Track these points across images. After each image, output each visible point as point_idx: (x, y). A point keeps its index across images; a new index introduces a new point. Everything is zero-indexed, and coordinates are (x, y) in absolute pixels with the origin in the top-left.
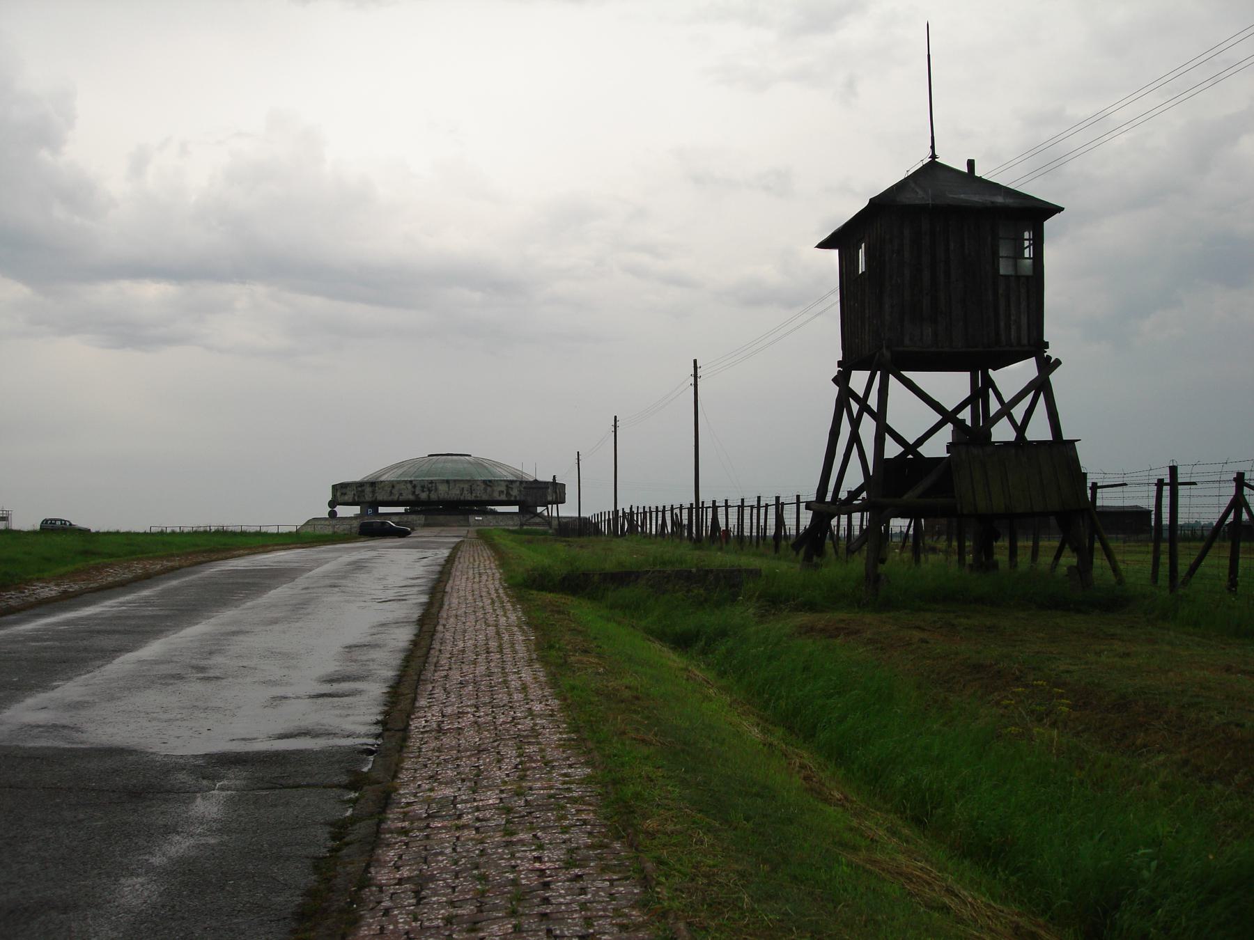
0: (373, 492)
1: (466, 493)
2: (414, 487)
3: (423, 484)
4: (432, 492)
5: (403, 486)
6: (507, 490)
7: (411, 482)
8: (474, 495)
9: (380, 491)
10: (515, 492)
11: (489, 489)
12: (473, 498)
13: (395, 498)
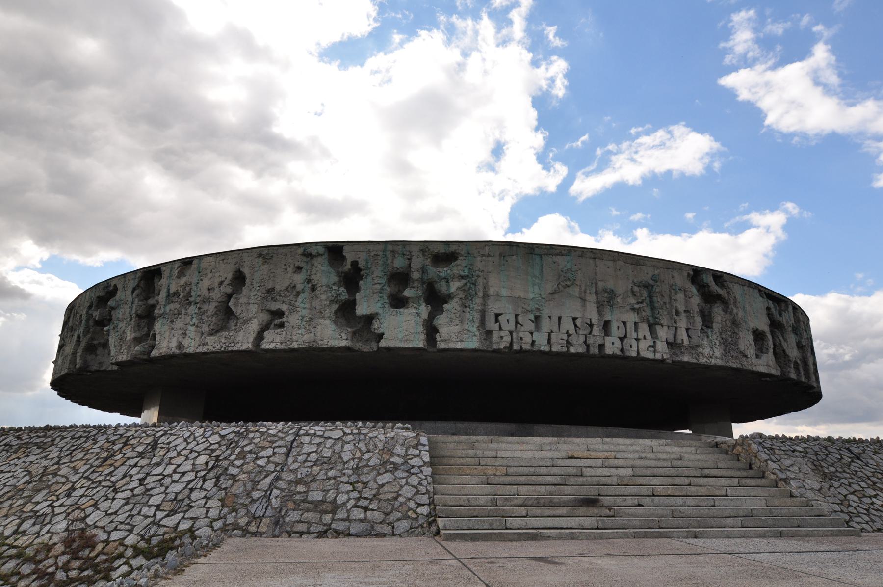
0: (147, 317)
1: (632, 318)
3: (399, 263)
8: (663, 333)
12: (662, 351)
13: (243, 341)
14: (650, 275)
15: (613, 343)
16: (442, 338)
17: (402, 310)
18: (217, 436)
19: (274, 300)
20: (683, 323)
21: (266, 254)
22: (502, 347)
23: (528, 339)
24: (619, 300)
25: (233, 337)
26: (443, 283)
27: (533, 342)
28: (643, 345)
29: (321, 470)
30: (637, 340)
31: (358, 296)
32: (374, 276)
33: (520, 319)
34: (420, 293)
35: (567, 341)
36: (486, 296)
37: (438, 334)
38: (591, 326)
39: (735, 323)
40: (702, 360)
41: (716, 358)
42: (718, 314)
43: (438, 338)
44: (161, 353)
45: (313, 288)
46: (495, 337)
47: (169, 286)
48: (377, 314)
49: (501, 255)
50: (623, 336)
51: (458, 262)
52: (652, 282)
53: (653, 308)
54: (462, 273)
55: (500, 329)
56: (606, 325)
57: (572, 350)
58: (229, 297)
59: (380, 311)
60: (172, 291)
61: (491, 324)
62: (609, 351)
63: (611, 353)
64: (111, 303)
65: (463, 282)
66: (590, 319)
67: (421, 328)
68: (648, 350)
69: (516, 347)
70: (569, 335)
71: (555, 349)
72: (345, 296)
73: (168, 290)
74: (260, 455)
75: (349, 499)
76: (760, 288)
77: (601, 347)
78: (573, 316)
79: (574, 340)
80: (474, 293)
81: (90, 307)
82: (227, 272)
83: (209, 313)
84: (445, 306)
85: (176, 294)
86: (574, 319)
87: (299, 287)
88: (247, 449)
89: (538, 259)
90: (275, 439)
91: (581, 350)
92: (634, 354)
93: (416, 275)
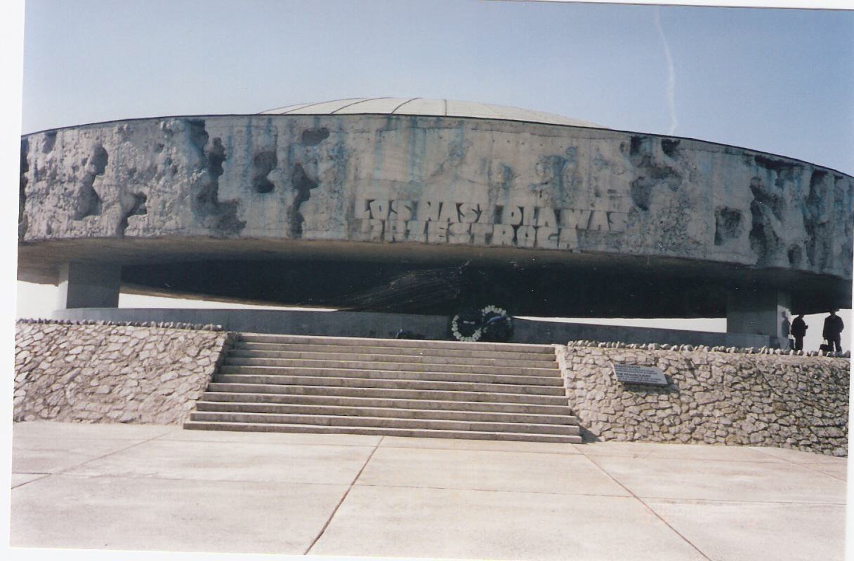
1: (529, 201)
6: (755, 210)
7: (196, 125)
8: (571, 219)
9: (42, 184)
10: (789, 229)
12: (570, 238)
14: (565, 147)
15: (504, 233)
16: (307, 228)
17: (268, 195)
18: (41, 333)
19: (136, 182)
22: (372, 238)
23: (401, 227)
24: (517, 181)
25: (97, 223)
26: (311, 165)
27: (407, 233)
28: (544, 233)
29: (117, 367)
30: (536, 228)
31: (221, 179)
32: (237, 156)
33: (394, 206)
34: (285, 177)
35: (448, 229)
36: (356, 178)
37: (303, 223)
38: (479, 212)
39: (686, 203)
40: (625, 249)
41: (647, 246)
42: (661, 195)
43: (303, 228)
44: (33, 237)
45: (175, 171)
46: (364, 227)
47: (36, 161)
48: (239, 199)
49: (377, 131)
50: (517, 222)
51: (329, 139)
52: (566, 157)
53: (562, 189)
54: (331, 154)
55: (371, 217)
56: (499, 211)
57: (453, 240)
58: (93, 176)
59: (243, 197)
60: (39, 168)
61: (361, 212)
62: (497, 241)
63: (500, 243)
65: (332, 163)
66: (478, 206)
67: (284, 216)
68: (549, 238)
69: (388, 237)
70: (450, 225)
71: (432, 239)
73: (36, 168)
74: (71, 352)
75: (131, 392)
76: (746, 152)
77: (489, 237)
78: (459, 201)
79: (456, 228)
80: (343, 176)
82: (86, 148)
83: (75, 194)
84: (312, 191)
85: (44, 171)
86: (458, 206)
87: (160, 168)
88: (62, 346)
89: (419, 133)
90: (88, 337)
91: (463, 240)
92: (530, 244)
93: (281, 156)
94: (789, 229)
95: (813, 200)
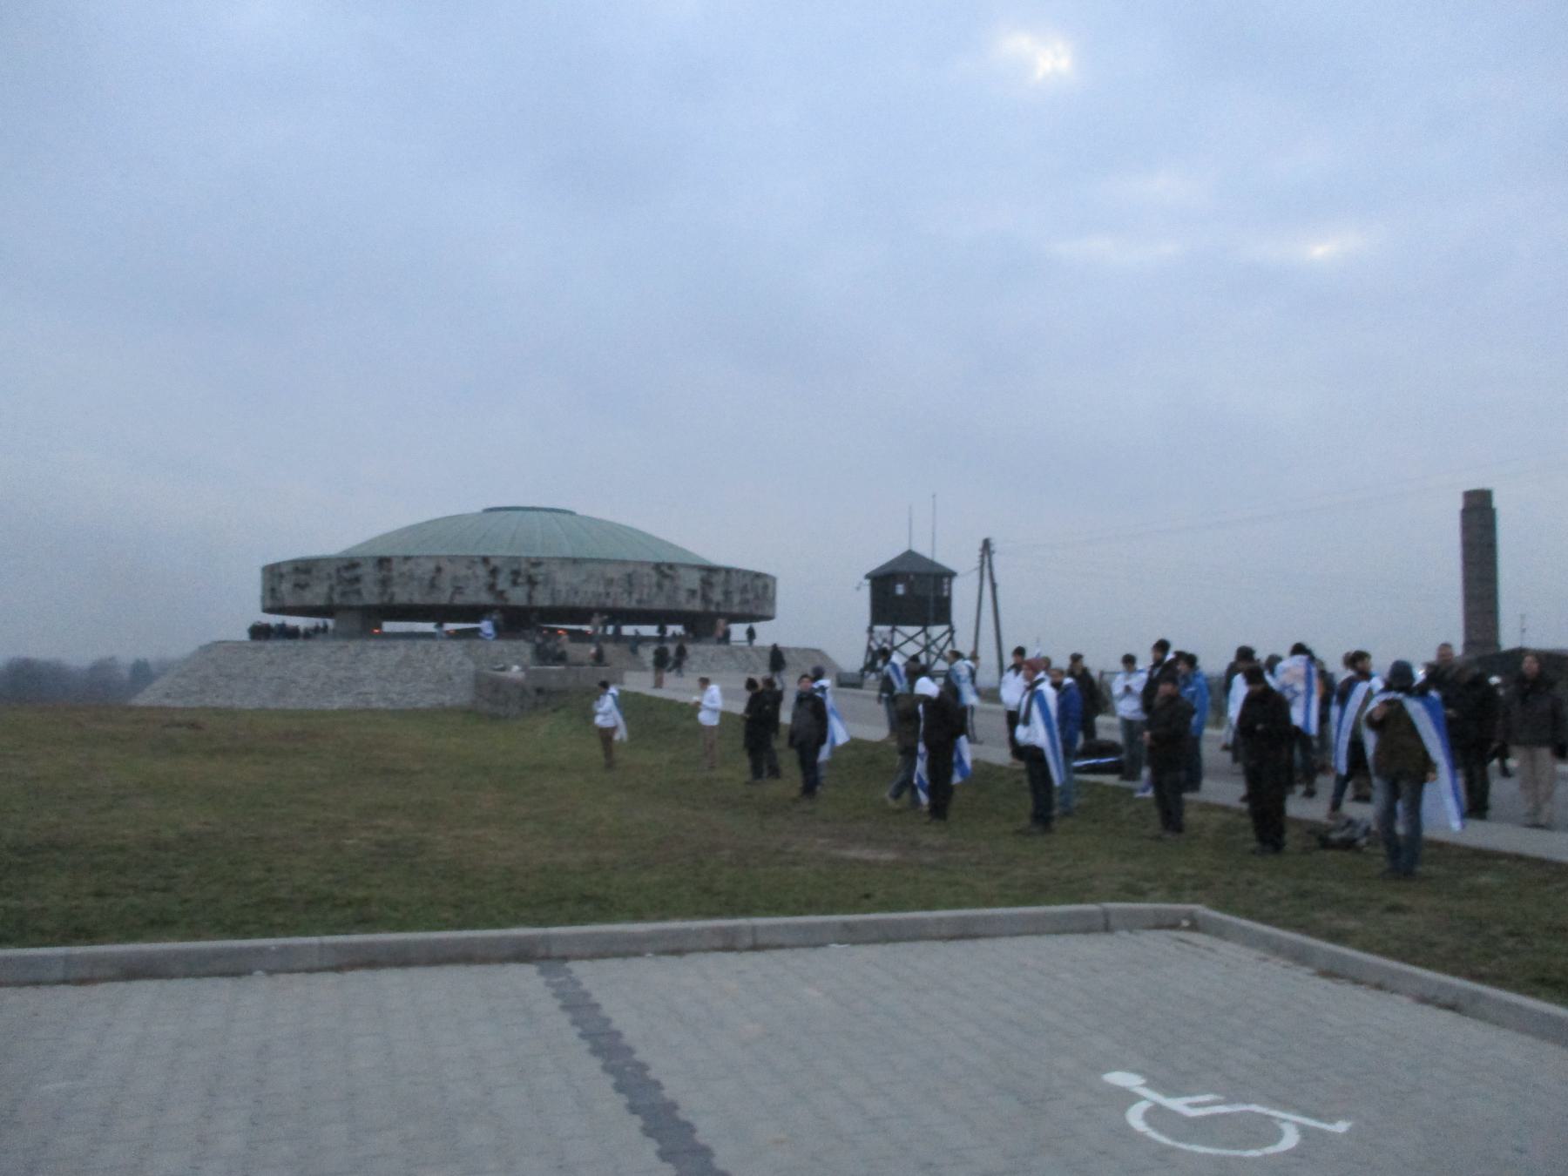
0: (385, 583)
2: (494, 572)
3: (515, 567)
4: (540, 588)
5: (463, 572)
6: (703, 589)
7: (485, 560)
8: (636, 596)
11: (667, 583)
20: (646, 591)
21: (452, 559)
42: (667, 583)
64: (359, 571)
72: (491, 580)
81: (338, 570)
82: (431, 565)
94: (717, 595)
95: (727, 581)
